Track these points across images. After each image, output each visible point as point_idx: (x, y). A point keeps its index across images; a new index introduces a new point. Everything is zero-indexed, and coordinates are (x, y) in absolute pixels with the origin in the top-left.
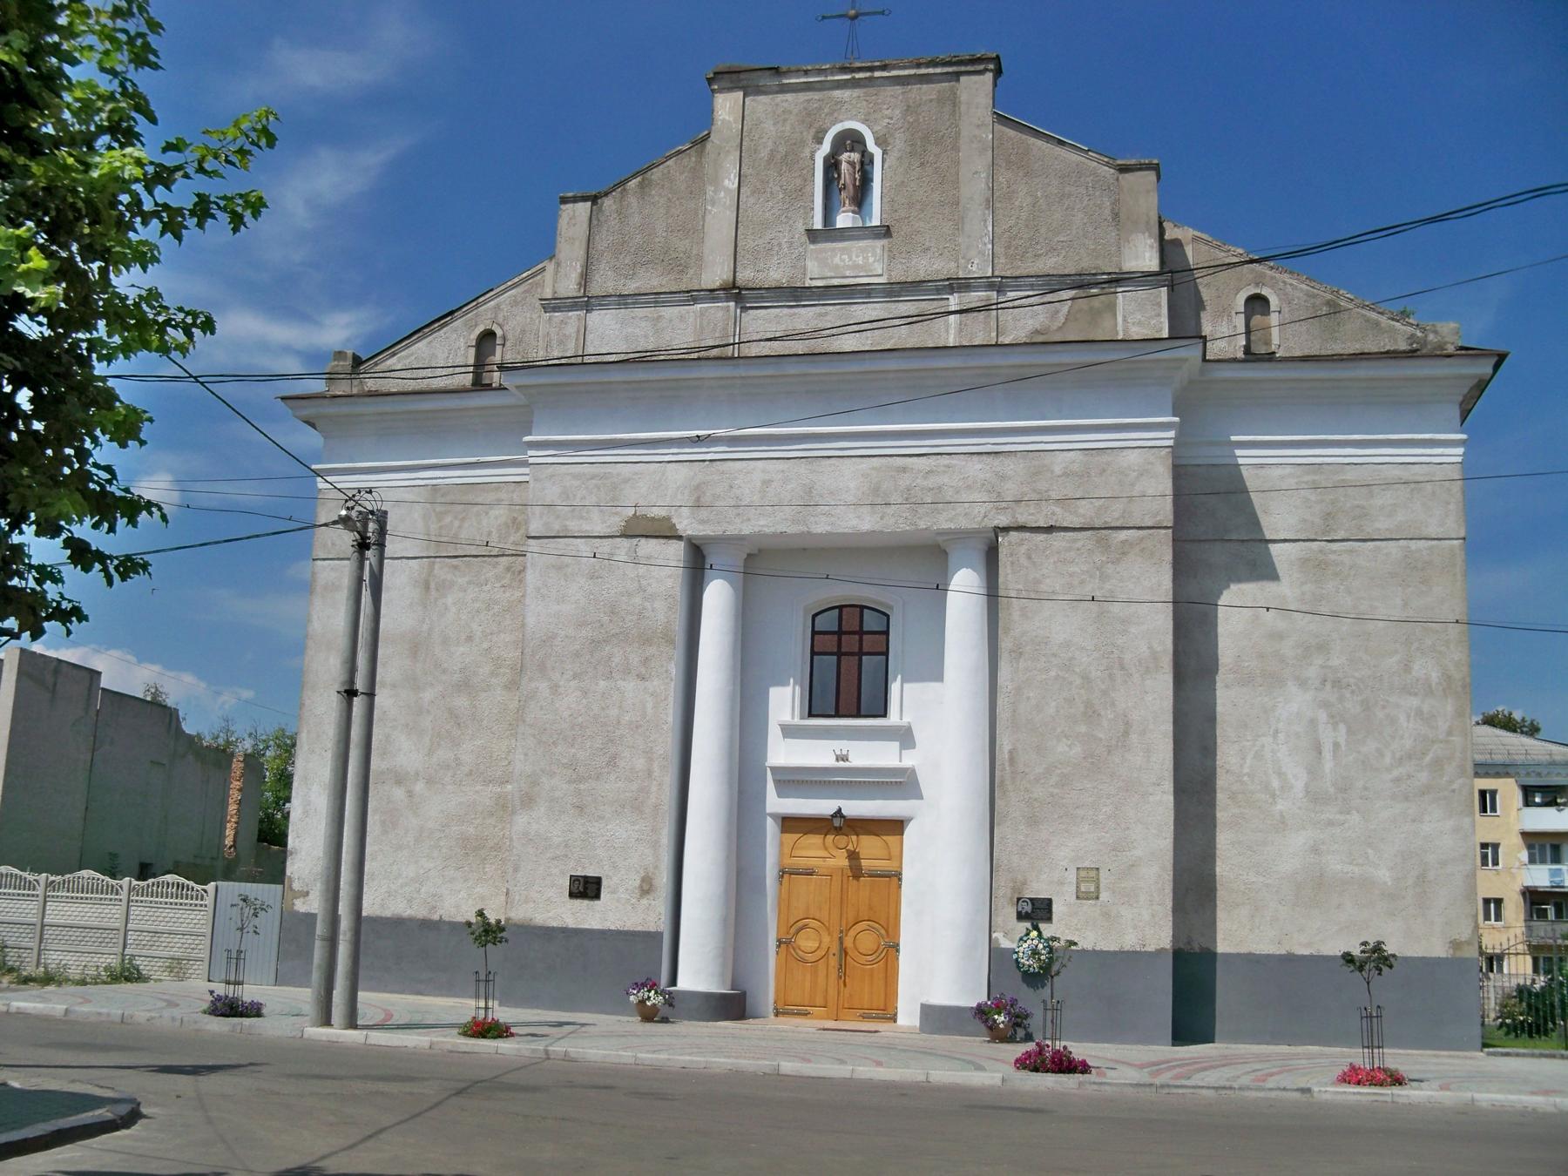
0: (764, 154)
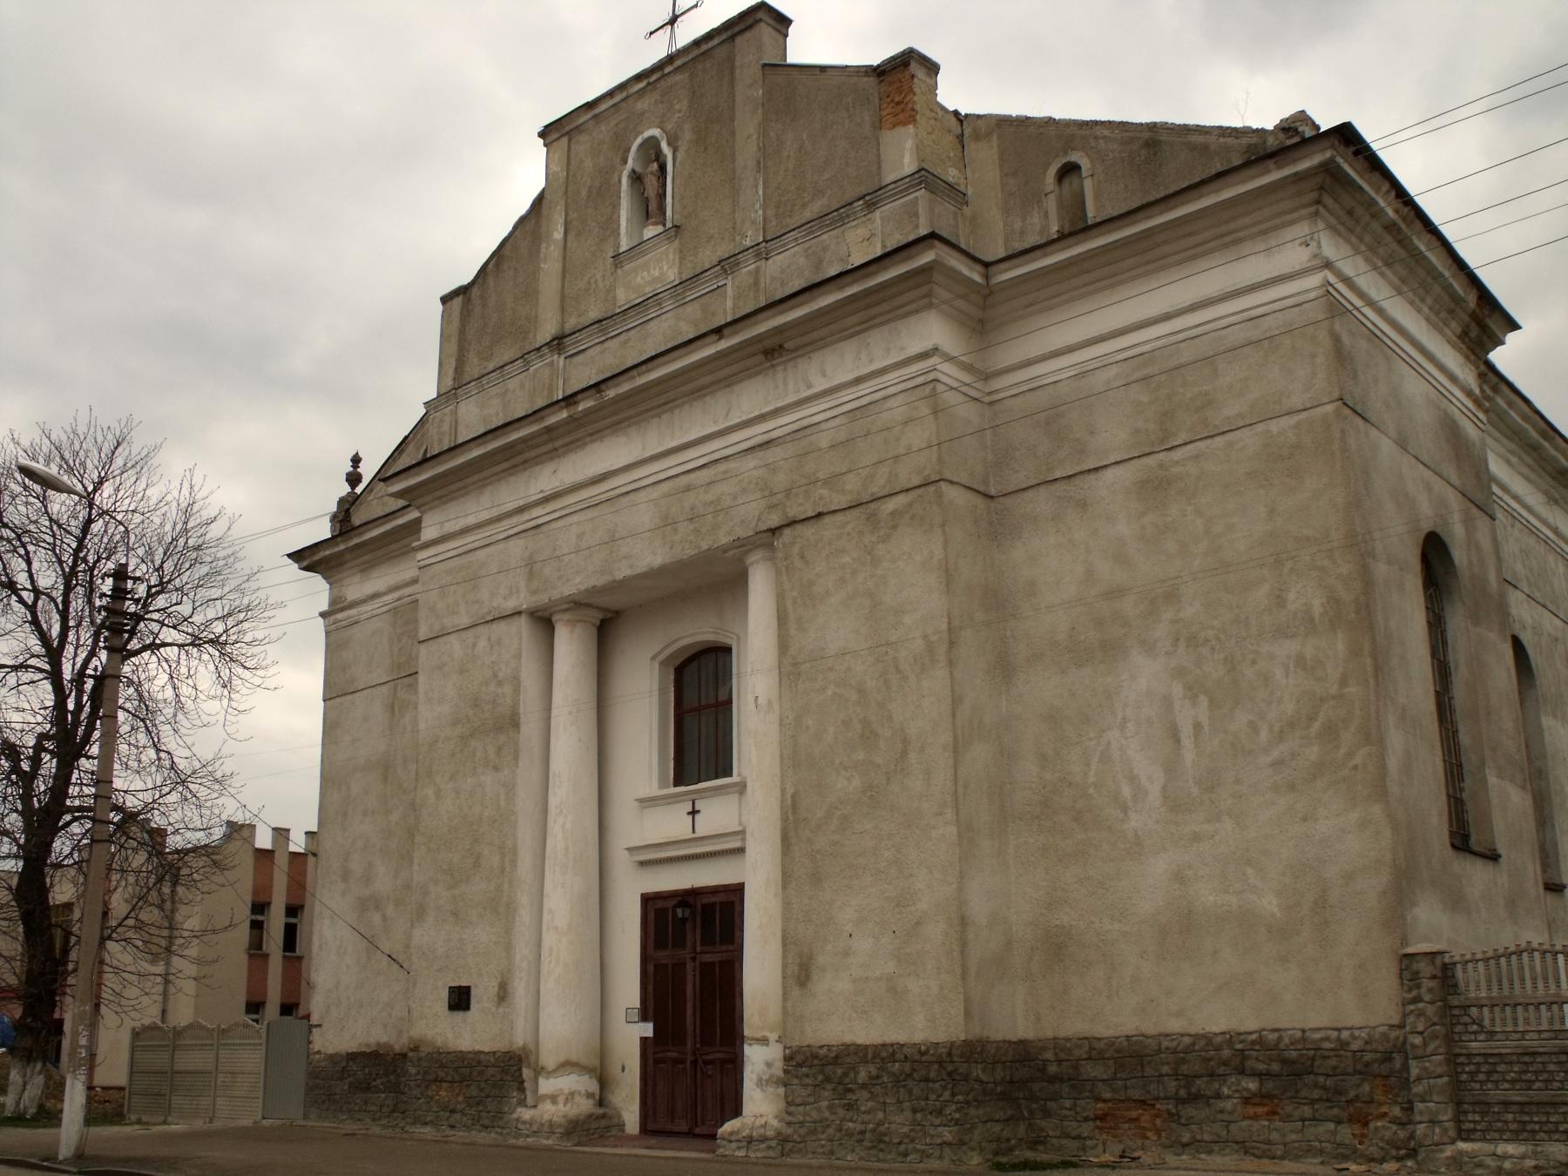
0: (584, 193)
